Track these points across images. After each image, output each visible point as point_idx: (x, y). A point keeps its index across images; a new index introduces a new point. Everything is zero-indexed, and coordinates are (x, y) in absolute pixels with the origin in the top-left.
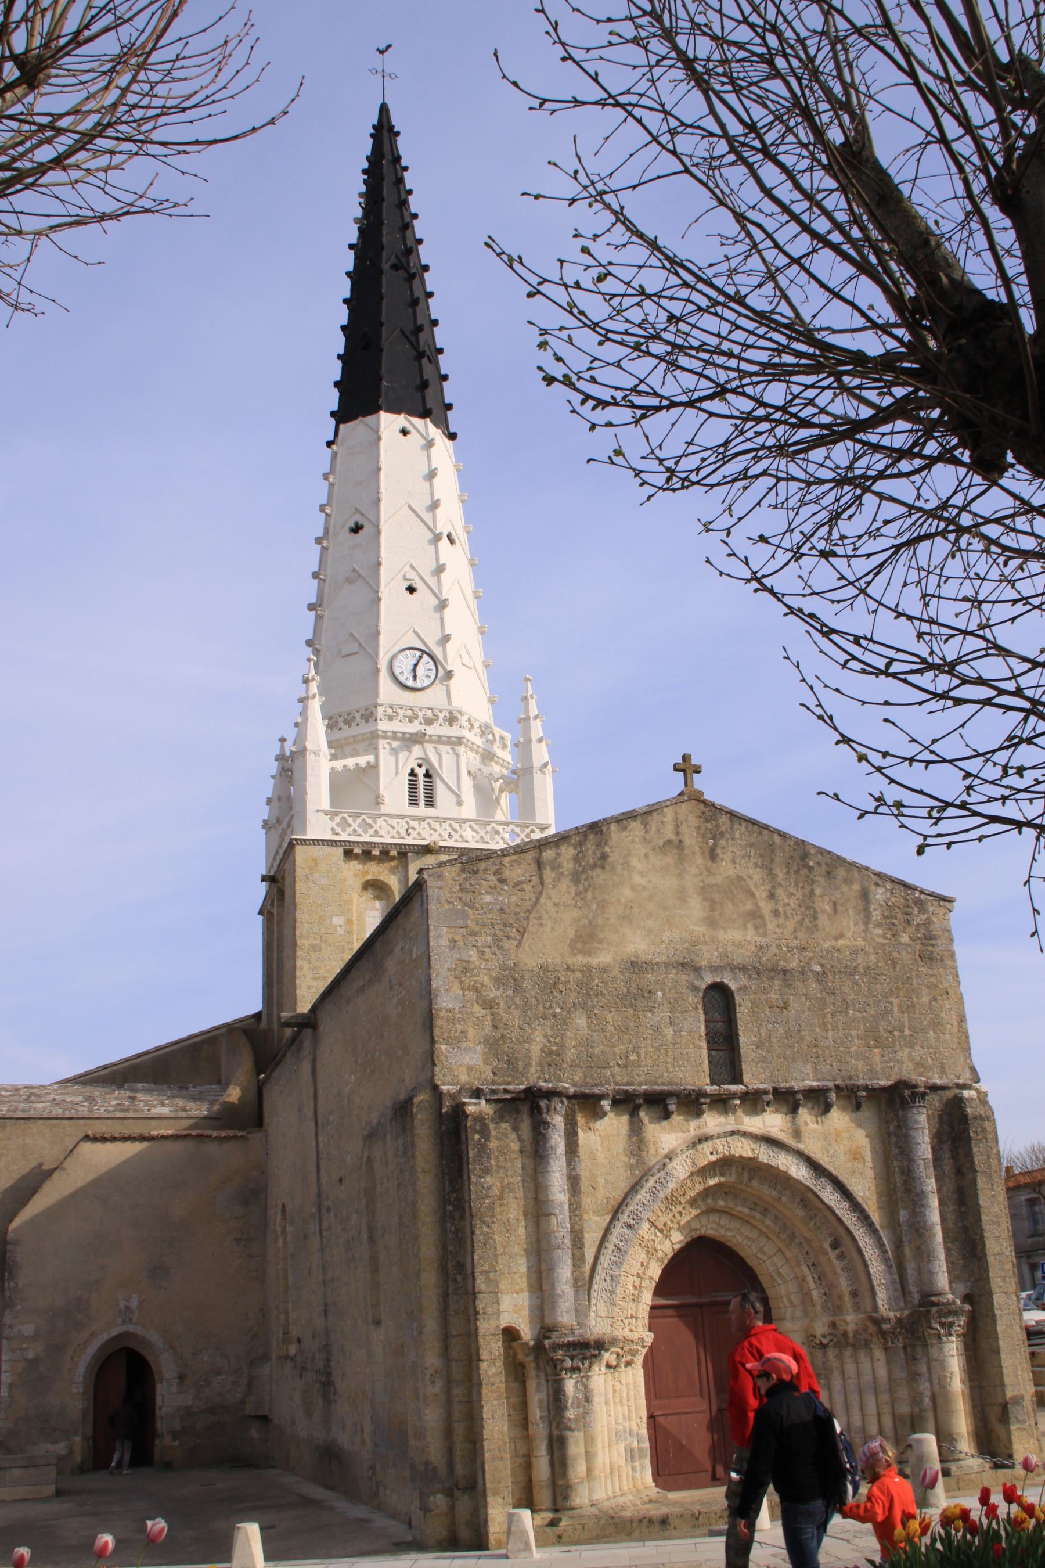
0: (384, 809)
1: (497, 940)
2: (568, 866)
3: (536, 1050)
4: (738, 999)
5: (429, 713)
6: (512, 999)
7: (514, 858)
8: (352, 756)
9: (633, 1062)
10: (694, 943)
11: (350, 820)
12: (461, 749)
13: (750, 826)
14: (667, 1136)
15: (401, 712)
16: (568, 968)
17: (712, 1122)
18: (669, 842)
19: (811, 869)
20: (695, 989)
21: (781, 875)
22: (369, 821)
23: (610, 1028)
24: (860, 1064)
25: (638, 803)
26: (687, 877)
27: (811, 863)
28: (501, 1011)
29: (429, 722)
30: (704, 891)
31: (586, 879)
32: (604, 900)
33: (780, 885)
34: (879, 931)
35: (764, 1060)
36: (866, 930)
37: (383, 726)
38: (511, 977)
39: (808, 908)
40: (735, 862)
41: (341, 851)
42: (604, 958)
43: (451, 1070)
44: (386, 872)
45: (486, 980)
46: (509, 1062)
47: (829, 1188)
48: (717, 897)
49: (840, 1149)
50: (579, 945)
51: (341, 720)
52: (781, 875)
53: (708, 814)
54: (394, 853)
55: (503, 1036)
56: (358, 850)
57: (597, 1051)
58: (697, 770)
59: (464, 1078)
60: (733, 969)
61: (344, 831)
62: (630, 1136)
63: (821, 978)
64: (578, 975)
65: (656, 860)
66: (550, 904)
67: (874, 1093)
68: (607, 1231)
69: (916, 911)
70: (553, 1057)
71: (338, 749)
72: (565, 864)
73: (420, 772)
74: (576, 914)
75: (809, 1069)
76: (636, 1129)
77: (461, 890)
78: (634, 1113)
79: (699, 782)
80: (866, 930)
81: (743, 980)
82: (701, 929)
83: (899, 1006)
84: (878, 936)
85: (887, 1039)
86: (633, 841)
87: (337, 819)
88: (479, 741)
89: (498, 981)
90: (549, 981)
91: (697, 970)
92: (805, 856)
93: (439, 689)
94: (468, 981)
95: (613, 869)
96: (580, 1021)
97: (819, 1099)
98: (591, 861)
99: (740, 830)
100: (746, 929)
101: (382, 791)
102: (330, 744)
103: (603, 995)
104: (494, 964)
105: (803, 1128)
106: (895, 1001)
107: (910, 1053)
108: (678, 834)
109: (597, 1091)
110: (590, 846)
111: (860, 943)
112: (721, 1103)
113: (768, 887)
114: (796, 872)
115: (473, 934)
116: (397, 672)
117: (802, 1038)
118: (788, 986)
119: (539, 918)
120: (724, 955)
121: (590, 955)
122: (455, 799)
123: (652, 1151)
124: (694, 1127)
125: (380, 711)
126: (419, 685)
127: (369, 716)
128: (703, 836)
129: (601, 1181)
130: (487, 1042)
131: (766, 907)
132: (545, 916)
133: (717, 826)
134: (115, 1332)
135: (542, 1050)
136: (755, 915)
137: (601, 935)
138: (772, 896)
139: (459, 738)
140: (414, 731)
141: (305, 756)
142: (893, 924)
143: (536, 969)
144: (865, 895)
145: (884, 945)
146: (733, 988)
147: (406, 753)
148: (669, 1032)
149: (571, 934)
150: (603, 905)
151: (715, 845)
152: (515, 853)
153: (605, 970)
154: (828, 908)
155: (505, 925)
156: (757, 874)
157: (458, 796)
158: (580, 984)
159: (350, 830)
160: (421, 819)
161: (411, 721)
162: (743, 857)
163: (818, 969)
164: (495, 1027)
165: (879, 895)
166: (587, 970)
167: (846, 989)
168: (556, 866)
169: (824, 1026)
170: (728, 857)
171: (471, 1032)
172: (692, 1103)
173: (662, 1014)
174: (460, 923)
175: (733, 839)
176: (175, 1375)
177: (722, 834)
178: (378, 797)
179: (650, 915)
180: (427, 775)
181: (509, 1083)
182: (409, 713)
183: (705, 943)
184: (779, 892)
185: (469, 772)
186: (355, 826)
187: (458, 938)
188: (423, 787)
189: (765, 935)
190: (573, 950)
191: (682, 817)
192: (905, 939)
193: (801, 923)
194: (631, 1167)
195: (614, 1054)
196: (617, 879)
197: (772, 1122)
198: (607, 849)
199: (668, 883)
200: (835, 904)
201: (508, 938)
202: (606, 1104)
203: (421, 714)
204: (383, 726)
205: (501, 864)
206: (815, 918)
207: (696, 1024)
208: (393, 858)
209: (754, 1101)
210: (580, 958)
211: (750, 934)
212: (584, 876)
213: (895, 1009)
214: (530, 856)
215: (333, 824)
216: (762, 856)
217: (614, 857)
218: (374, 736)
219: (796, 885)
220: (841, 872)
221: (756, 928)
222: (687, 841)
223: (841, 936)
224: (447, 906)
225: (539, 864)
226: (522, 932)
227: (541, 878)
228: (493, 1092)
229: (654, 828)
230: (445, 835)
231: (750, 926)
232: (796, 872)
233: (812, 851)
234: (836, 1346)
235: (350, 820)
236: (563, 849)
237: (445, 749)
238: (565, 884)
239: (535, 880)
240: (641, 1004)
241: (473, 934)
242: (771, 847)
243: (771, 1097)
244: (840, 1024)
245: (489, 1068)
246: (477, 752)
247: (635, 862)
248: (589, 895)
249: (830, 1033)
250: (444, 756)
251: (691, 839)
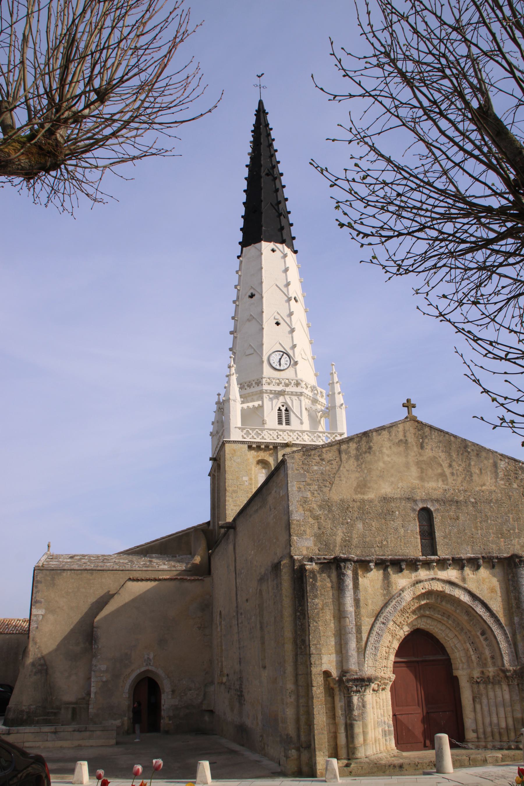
0: (266, 426)
1: (320, 487)
2: (353, 452)
3: (339, 539)
4: (434, 515)
5: (287, 381)
6: (327, 515)
7: (328, 449)
8: (251, 402)
9: (385, 545)
10: (413, 489)
11: (251, 431)
12: (302, 398)
13: (439, 433)
14: (402, 581)
15: (274, 381)
16: (354, 500)
17: (423, 573)
18: (401, 440)
19: (469, 453)
20: (414, 510)
22: (260, 432)
23: (374, 529)
24: (494, 546)
25: (386, 422)
26: (410, 457)
27: (469, 450)
28: (322, 521)
29: (287, 385)
30: (418, 464)
31: (362, 459)
32: (370, 468)
33: (454, 460)
34: (502, 482)
35: (447, 544)
36: (496, 482)
37: (265, 387)
38: (327, 505)
39: (468, 471)
40: (433, 450)
41: (246, 446)
42: (370, 496)
43: (298, 549)
44: (268, 456)
45: (315, 506)
46: (326, 545)
47: (480, 606)
48: (424, 466)
49: (485, 587)
50: (359, 490)
51: (246, 385)
53: (419, 427)
54: (271, 447)
55: (323, 532)
56: (254, 446)
57: (367, 540)
58: (414, 406)
59: (305, 552)
60: (432, 500)
61: (248, 436)
62: (383, 580)
63: (474, 505)
64: (358, 504)
65: (395, 449)
66: (345, 470)
67: (501, 560)
68: (373, 626)
69: (520, 472)
70: (347, 543)
71: (245, 398)
72: (351, 452)
73: (283, 409)
74: (357, 475)
75: (469, 548)
76: (386, 577)
77: (303, 464)
78: (385, 569)
79: (415, 412)
80: (496, 482)
81: (437, 506)
82: (417, 482)
83: (513, 518)
84: (502, 484)
85: (507, 534)
86: (384, 440)
87: (245, 431)
88: (310, 394)
89: (320, 507)
90: (345, 507)
91: (415, 501)
92: (466, 447)
93: (291, 370)
94: (307, 507)
95: (375, 453)
96: (360, 525)
97: (474, 563)
98: (364, 450)
99: (435, 434)
100: (438, 481)
101: (265, 418)
102: (241, 396)
103: (370, 513)
104: (318, 499)
105: (466, 577)
106: (511, 516)
107: (518, 541)
108: (405, 436)
109: (368, 558)
110: (363, 443)
111: (493, 488)
112: (427, 565)
113: (448, 462)
114: (462, 454)
115: (309, 485)
116: (272, 362)
117: (466, 534)
118: (459, 509)
119: (340, 477)
120: (428, 494)
121: (364, 494)
122: (299, 421)
123: (394, 588)
124: (414, 576)
125: (264, 381)
126: (282, 368)
127: (259, 383)
128: (417, 437)
129: (370, 602)
130: (315, 535)
131: (448, 471)
132: (342, 476)
133: (424, 433)
134: (143, 669)
135: (342, 539)
136: (443, 475)
137: (369, 485)
138: (450, 466)
139: (301, 393)
140: (280, 390)
141: (229, 402)
142: (509, 479)
143: (339, 501)
145: (505, 489)
146: (432, 510)
147: (276, 400)
148: (402, 531)
149: (355, 484)
150: (370, 470)
151: (423, 442)
152: (328, 446)
153: (371, 501)
154: (477, 471)
155: (324, 480)
156: (443, 456)
157: (301, 420)
158: (359, 508)
159: (250, 436)
160: (284, 431)
161: (278, 385)
162: (436, 447)
163: (473, 500)
164: (319, 528)
165: (502, 465)
166: (363, 501)
167: (486, 510)
168: (347, 452)
169: (476, 528)
170: (429, 447)
171: (308, 531)
172: (413, 565)
173: (398, 522)
174: (303, 479)
175: (431, 439)
176: (170, 690)
177: (426, 436)
178: (263, 420)
179: (392, 475)
180: (286, 410)
181: (326, 555)
182: (278, 381)
183: (419, 488)
184: (454, 464)
185: (306, 409)
186: (253, 434)
187: (301, 486)
188: (284, 416)
189: (447, 484)
190: (356, 491)
191: (407, 429)
192: (515, 486)
193: (465, 479)
194: (384, 595)
195: (376, 541)
196: (376, 458)
197: (452, 574)
198: (371, 444)
199: (400, 460)
200: (481, 470)
201: (325, 486)
202: (372, 565)
203: (283, 382)
204: (265, 387)
205: (322, 452)
206: (472, 476)
207: (415, 527)
208: (271, 449)
209: (443, 564)
210: (359, 496)
211: (440, 484)
212: (361, 457)
213: (511, 520)
214: (335, 448)
215: (243, 434)
216: (445, 447)
217: (375, 448)
218: (261, 392)
219: (462, 460)
220: (484, 454)
221: (443, 481)
222: (410, 440)
223: (484, 485)
224: (296, 472)
225: (340, 452)
226: (332, 484)
227: (341, 458)
228: (318, 559)
229: (394, 434)
230: (295, 438)
231: (440, 480)
232: (462, 454)
233: (470, 444)
234: (484, 683)
235: (251, 431)
236: (351, 444)
237: (294, 398)
238: (352, 461)
239: (338, 459)
240: (388, 517)
241: (309, 485)
242: (450, 442)
243: (451, 562)
244: (484, 527)
245: (317, 548)
246: (309, 399)
247: (385, 450)
248: (363, 466)
249: (479, 531)
250: (294, 401)
251: (411, 439)
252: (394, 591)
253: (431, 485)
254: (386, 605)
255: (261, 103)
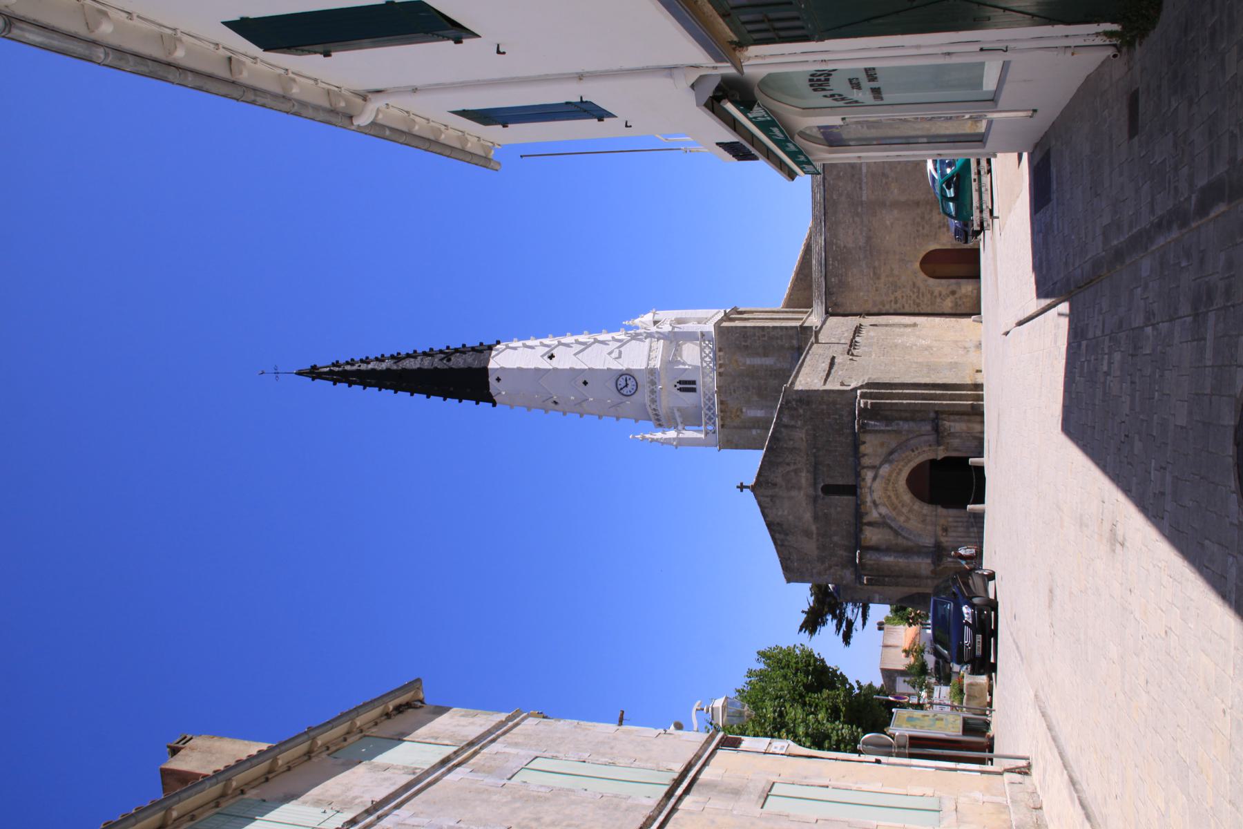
2: (782, 536)
21: (780, 460)
38: (821, 560)
42: (814, 528)
52: (780, 460)
60: (815, 484)
73: (679, 386)
89: (823, 562)
96: (835, 539)
131: (792, 467)
138: (788, 464)
144: (786, 426)
156: (780, 470)
165: (785, 420)
168: (782, 540)
211: (803, 474)
251: (770, 492)
252: (880, 520)
253: (803, 481)
254: (891, 528)
255: (300, 373)
